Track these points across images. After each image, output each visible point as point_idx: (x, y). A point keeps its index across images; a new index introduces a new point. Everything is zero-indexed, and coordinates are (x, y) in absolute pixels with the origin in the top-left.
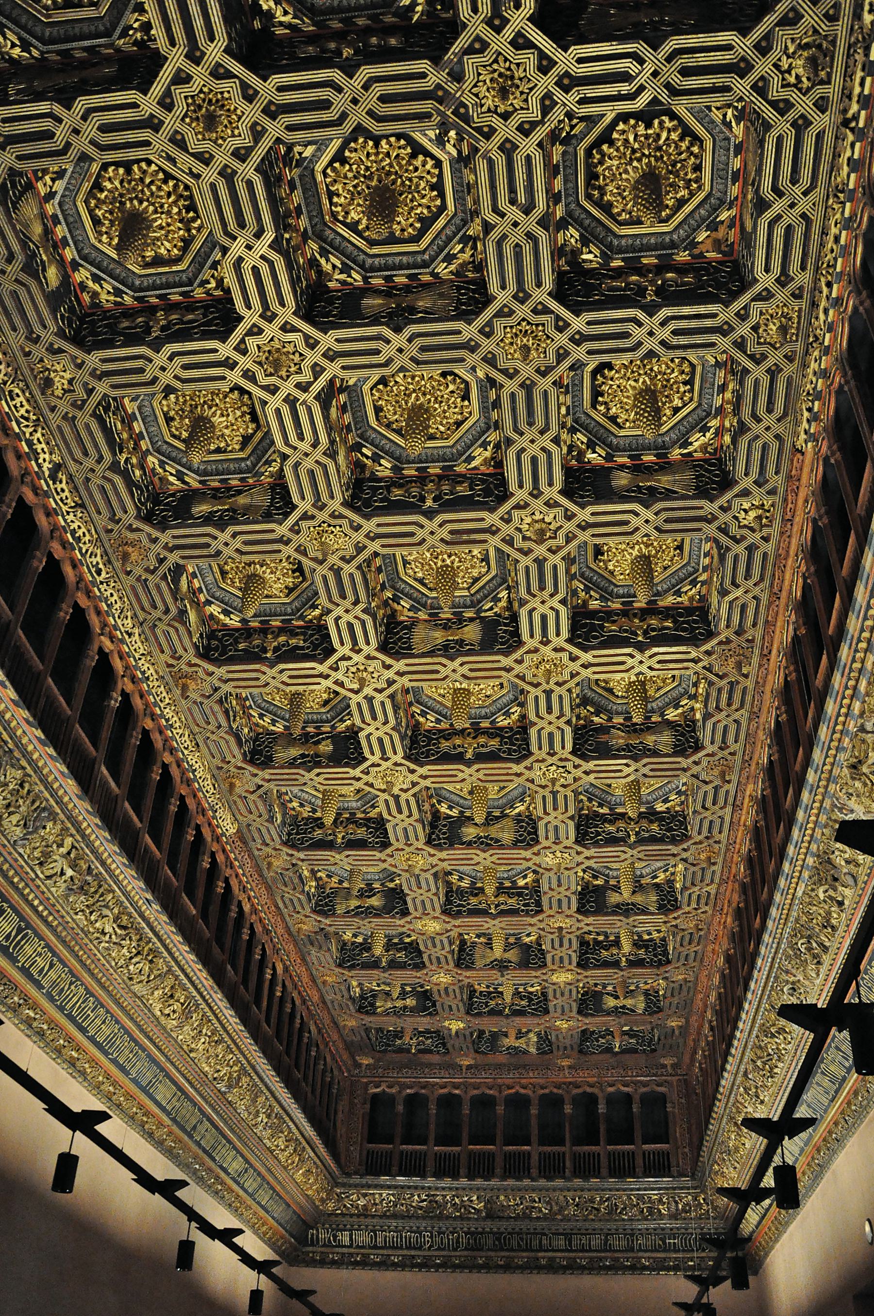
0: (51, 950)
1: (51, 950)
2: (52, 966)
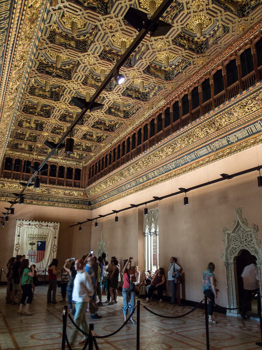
0: (151, 172)
1: (151, 172)
2: (154, 173)
